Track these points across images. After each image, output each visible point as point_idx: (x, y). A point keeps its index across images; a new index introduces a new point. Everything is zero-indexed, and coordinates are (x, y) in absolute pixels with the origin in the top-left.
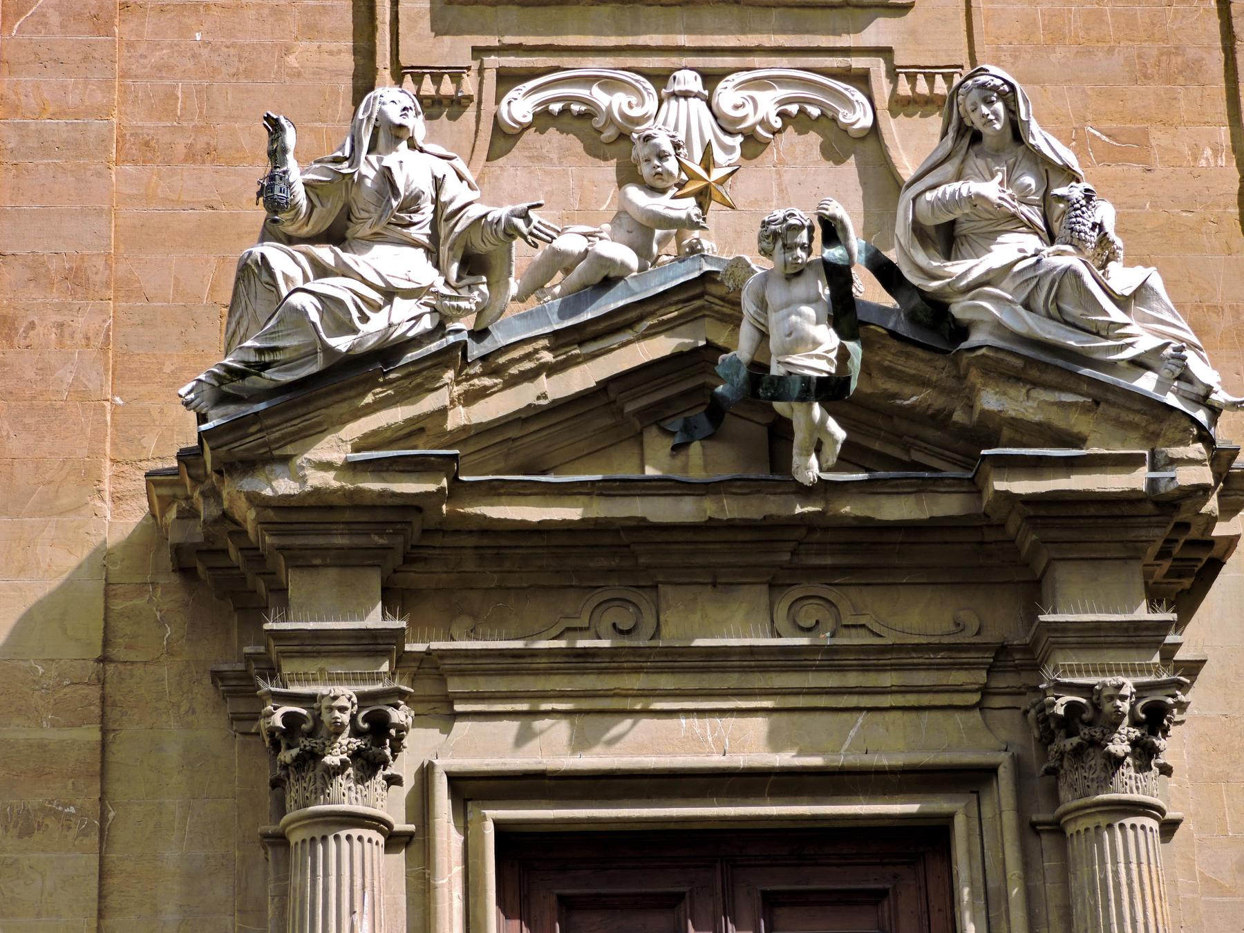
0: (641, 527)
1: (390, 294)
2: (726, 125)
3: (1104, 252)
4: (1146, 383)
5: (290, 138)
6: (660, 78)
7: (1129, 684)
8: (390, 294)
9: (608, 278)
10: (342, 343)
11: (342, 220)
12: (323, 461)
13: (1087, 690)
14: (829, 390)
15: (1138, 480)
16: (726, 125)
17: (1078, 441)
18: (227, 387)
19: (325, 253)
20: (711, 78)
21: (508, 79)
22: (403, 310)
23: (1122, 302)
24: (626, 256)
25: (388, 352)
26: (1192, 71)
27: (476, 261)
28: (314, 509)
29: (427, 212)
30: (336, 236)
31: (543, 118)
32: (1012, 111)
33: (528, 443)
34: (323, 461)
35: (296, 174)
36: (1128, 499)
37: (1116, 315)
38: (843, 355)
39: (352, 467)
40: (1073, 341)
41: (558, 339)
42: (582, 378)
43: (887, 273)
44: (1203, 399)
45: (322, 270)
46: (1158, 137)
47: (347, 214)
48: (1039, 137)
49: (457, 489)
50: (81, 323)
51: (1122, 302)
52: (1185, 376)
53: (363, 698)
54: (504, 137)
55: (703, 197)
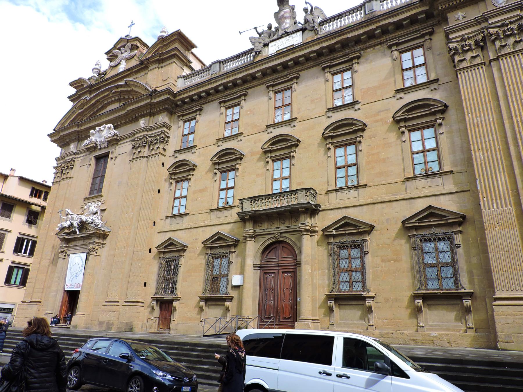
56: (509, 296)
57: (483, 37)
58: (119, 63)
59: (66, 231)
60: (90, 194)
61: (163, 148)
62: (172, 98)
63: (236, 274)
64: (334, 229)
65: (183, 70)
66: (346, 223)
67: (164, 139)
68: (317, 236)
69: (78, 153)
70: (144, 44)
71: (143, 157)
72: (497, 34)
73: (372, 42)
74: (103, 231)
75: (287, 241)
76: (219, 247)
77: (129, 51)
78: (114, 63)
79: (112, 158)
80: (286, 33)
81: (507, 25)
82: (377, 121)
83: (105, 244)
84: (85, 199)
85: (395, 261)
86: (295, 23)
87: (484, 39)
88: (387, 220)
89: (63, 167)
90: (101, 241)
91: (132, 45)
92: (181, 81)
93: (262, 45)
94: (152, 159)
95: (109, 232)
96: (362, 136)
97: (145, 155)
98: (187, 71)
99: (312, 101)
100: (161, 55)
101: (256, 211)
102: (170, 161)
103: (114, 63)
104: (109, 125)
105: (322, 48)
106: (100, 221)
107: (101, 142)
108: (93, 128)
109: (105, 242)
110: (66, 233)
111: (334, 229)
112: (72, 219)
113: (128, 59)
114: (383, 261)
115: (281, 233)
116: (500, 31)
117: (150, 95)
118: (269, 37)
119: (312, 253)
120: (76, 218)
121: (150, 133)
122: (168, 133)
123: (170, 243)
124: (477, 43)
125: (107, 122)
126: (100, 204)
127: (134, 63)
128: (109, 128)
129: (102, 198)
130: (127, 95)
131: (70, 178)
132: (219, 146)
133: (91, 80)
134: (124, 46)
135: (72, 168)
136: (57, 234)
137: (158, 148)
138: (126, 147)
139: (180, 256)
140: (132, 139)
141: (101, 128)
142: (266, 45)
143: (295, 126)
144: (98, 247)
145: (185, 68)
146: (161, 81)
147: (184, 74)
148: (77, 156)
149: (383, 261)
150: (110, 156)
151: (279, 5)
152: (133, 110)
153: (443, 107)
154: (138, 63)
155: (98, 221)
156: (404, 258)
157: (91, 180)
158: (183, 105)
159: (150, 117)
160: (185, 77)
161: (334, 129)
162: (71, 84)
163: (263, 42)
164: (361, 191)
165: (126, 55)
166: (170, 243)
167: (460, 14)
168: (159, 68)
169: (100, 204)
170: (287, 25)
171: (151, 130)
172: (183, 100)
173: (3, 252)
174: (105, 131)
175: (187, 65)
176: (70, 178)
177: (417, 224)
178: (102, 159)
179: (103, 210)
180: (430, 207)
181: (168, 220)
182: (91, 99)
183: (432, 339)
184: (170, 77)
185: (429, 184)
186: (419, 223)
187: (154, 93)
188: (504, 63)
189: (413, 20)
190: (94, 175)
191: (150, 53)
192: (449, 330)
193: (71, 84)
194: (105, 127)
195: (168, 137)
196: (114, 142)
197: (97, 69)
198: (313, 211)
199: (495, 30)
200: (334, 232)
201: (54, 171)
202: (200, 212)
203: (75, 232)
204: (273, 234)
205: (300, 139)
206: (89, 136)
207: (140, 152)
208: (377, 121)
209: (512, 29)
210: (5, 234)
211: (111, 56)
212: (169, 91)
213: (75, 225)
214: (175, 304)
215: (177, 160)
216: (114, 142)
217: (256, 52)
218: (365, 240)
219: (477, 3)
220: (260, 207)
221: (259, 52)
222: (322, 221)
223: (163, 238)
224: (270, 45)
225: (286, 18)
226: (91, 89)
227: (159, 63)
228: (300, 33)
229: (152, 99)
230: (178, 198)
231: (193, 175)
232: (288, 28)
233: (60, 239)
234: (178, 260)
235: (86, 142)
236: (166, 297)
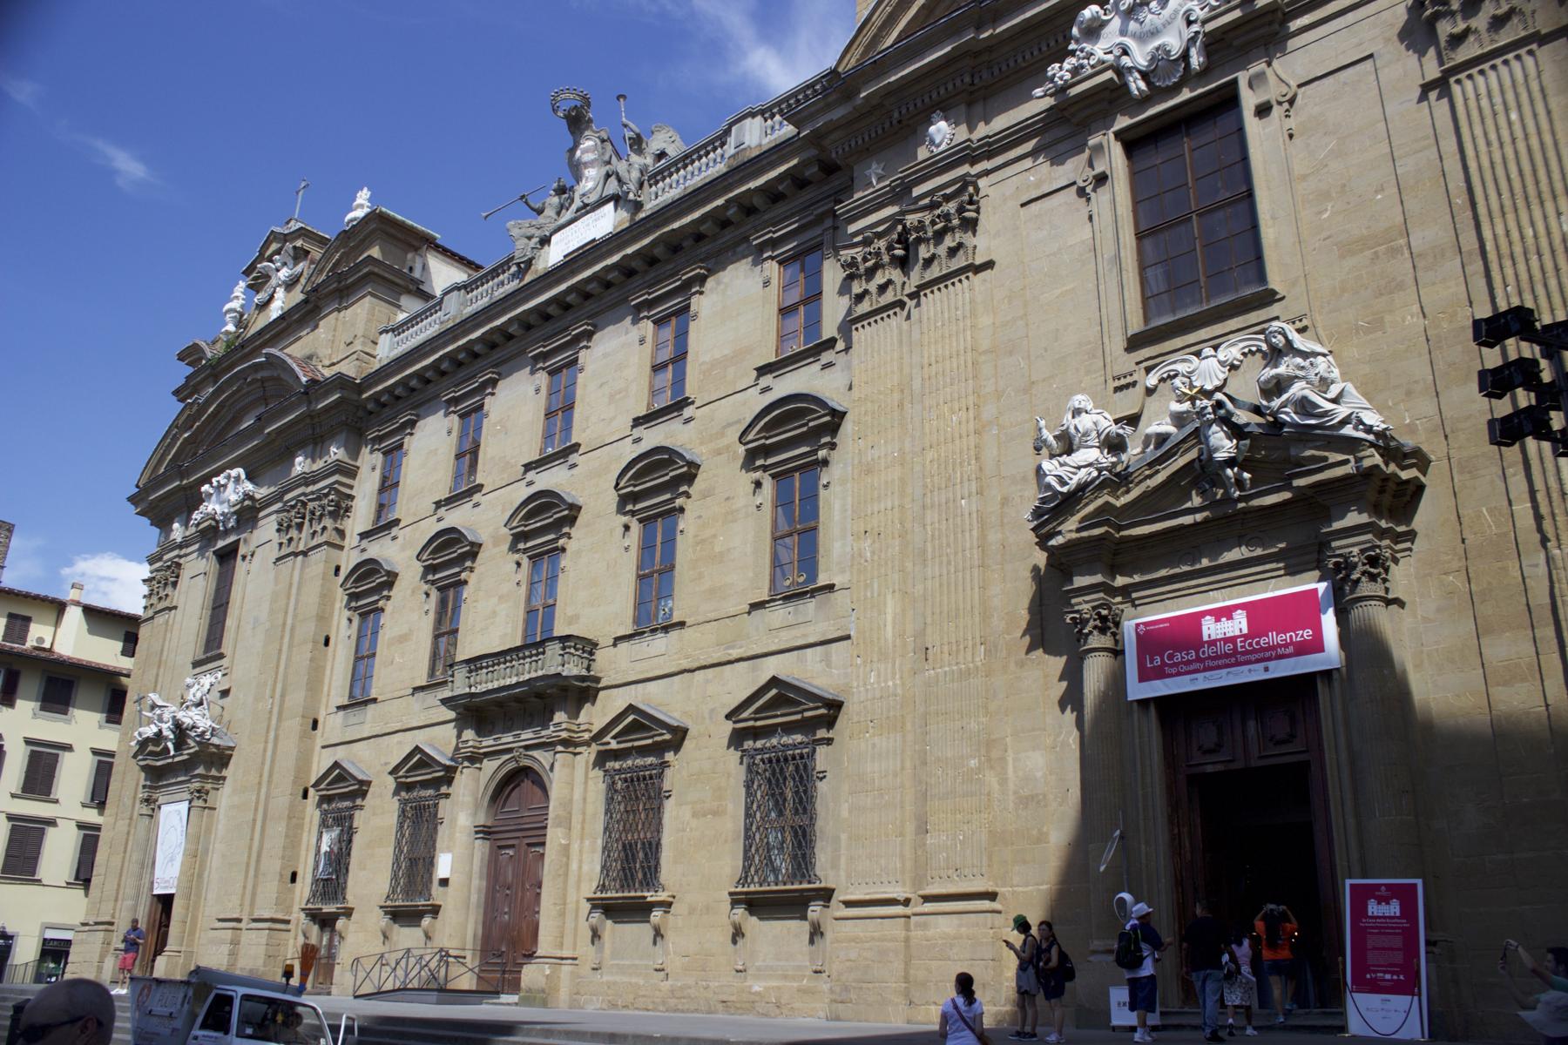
0: (1182, 527)
1: (1079, 468)
2: (1222, 363)
3: (1325, 383)
4: (1348, 430)
5: (1042, 423)
6: (1198, 354)
7: (1356, 550)
8: (1079, 468)
9: (1162, 438)
10: (1065, 489)
11: (1068, 444)
12: (1069, 529)
13: (1340, 556)
14: (1231, 462)
15: (1348, 469)
16: (1222, 363)
17: (1326, 459)
18: (1037, 513)
19: (1065, 458)
20: (1216, 348)
21: (1148, 370)
22: (1084, 471)
23: (1335, 401)
24: (1172, 429)
25: (1082, 487)
26: (1401, 287)
27: (1115, 445)
28: (1070, 545)
29: (1094, 434)
30: (1069, 451)
31: (1162, 380)
32: (1286, 337)
33: (1149, 505)
34: (1069, 529)
35: (1049, 436)
36: (1347, 477)
37: (1329, 406)
38: (1237, 447)
39: (1078, 530)
40: (1313, 422)
41: (1150, 465)
42: (1160, 478)
43: (1257, 410)
44: (1369, 429)
45: (1061, 465)
46: (1388, 318)
47: (1071, 444)
48: (1299, 342)
49: (1120, 528)
50: (1026, 494)
51: (1335, 401)
52: (1362, 423)
53: (1094, 608)
54: (1150, 392)
55: (1193, 399)
56: (868, 897)
57: (900, 235)
58: (271, 298)
59: (151, 748)
60: (206, 652)
61: (336, 529)
62: (355, 397)
63: (449, 850)
64: (614, 737)
65: (399, 307)
66: (637, 722)
67: (338, 506)
68: (589, 754)
69: (185, 544)
70: (322, 241)
71: (296, 554)
72: (921, 226)
73: (729, 235)
74: (217, 746)
75: (536, 766)
76: (422, 781)
77: (290, 262)
78: (261, 297)
79: (244, 558)
80: (586, 205)
81: (938, 205)
82: (718, 452)
83: (224, 778)
84: (196, 664)
85: (715, 813)
86: (608, 176)
87: (903, 240)
88: (712, 710)
89: (165, 578)
90: (214, 772)
91: (295, 248)
92: (386, 339)
93: (535, 240)
94: (315, 556)
95: (232, 749)
96: (689, 496)
97: (301, 548)
98: (411, 305)
99: (612, 397)
100: (341, 277)
101: (472, 695)
102: (349, 559)
103: (261, 297)
104: (234, 473)
105: (607, 269)
106: (209, 723)
107: (223, 514)
108: (207, 479)
109: (224, 773)
110: (152, 753)
111: (614, 737)
112: (161, 719)
113: (290, 285)
114: (695, 815)
115: (527, 748)
116: (927, 217)
117: (306, 393)
118: (558, 213)
119: (576, 791)
120: (166, 716)
121: (311, 488)
122: (351, 487)
123: (338, 773)
124: (890, 248)
125: (231, 466)
126: (219, 675)
127: (297, 296)
128: (237, 479)
129: (223, 662)
130: (273, 385)
131: (170, 609)
132: (439, 520)
133: (218, 345)
134: (278, 252)
135: (175, 584)
136: (135, 756)
137: (324, 528)
138: (267, 528)
139: (355, 807)
140: (278, 506)
141: (221, 479)
142: (545, 241)
143: (574, 466)
144: (208, 786)
145: (405, 301)
146: (343, 346)
147: (402, 317)
148: (183, 552)
149: (695, 815)
150: (242, 551)
151: (572, 133)
152: (279, 431)
153: (827, 418)
154: (302, 297)
155: (204, 723)
156: (730, 807)
157: (207, 613)
158: (369, 413)
159: (316, 444)
160: (397, 330)
161: (635, 477)
162: (181, 357)
163: (538, 233)
164: (674, 634)
165: (284, 273)
166: (338, 773)
167: (874, 170)
168: (339, 310)
169: (219, 675)
170: (590, 185)
171: (314, 483)
172: (375, 399)
173: (57, 801)
174: (231, 486)
175: (409, 292)
176: (170, 609)
177: (751, 723)
178: (227, 557)
179: (225, 693)
180: (774, 681)
181: (341, 713)
182: (208, 402)
183: (753, 998)
184: (357, 340)
185: (791, 619)
186: (756, 720)
187: (316, 387)
188: (931, 301)
189: (796, 180)
190: (215, 600)
191: (321, 271)
192: (785, 977)
193: (181, 357)
194: (229, 477)
195: (351, 497)
196: (248, 514)
197: (234, 310)
198: (582, 692)
199: (919, 216)
200: (614, 745)
201: (145, 590)
202: (397, 694)
203: (167, 749)
204: (510, 750)
205: (580, 501)
206: (199, 500)
207: (291, 540)
208: (718, 452)
209: (946, 217)
210: (57, 755)
211: (255, 279)
212: (341, 381)
213: (166, 733)
214: (340, 924)
215: (365, 556)
216: (248, 514)
217: (518, 265)
218: (665, 765)
219: (915, 132)
220: (486, 682)
221: (529, 263)
222: (596, 715)
223: (321, 763)
224: (554, 239)
225: (586, 165)
226: (215, 370)
227: (341, 298)
228: (611, 205)
229: (310, 403)
230: (362, 658)
231: (388, 598)
232: (590, 191)
233: (144, 768)
234: (351, 817)
235: (196, 516)
236: (329, 908)
